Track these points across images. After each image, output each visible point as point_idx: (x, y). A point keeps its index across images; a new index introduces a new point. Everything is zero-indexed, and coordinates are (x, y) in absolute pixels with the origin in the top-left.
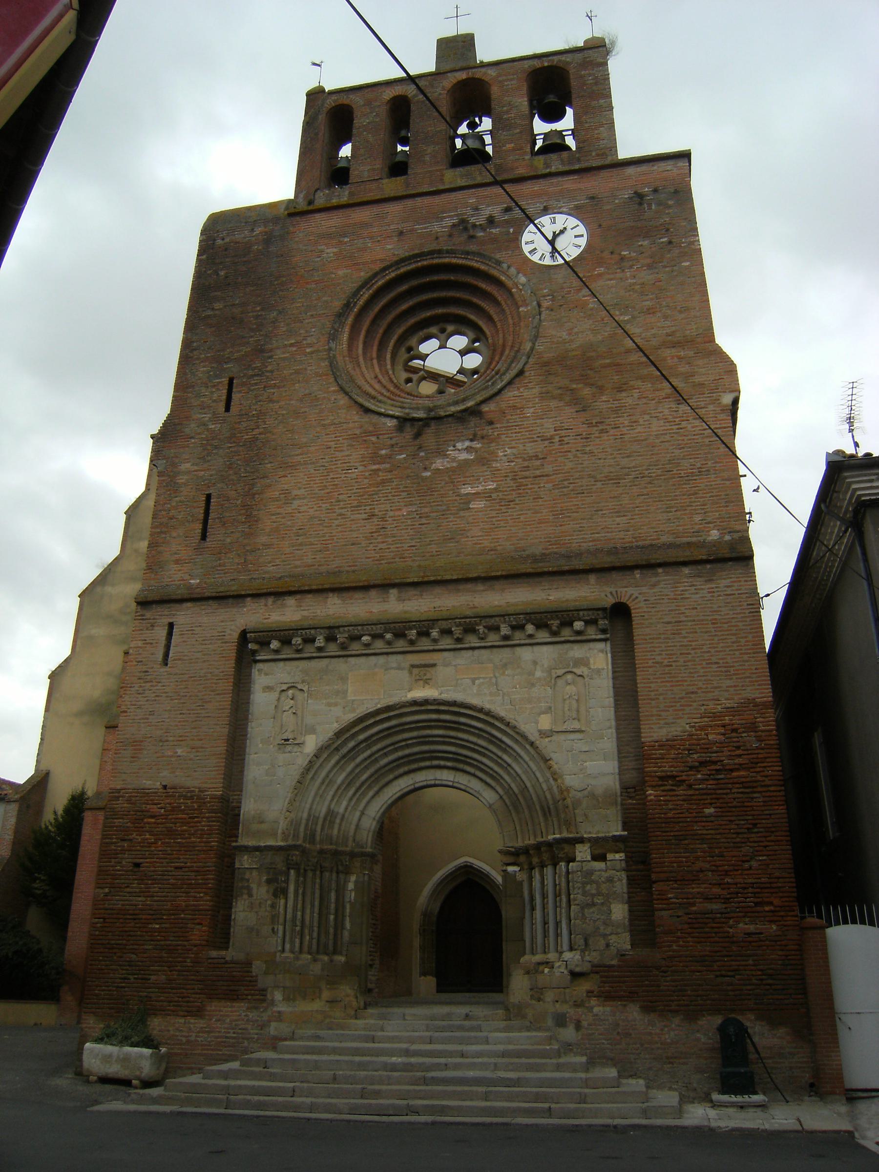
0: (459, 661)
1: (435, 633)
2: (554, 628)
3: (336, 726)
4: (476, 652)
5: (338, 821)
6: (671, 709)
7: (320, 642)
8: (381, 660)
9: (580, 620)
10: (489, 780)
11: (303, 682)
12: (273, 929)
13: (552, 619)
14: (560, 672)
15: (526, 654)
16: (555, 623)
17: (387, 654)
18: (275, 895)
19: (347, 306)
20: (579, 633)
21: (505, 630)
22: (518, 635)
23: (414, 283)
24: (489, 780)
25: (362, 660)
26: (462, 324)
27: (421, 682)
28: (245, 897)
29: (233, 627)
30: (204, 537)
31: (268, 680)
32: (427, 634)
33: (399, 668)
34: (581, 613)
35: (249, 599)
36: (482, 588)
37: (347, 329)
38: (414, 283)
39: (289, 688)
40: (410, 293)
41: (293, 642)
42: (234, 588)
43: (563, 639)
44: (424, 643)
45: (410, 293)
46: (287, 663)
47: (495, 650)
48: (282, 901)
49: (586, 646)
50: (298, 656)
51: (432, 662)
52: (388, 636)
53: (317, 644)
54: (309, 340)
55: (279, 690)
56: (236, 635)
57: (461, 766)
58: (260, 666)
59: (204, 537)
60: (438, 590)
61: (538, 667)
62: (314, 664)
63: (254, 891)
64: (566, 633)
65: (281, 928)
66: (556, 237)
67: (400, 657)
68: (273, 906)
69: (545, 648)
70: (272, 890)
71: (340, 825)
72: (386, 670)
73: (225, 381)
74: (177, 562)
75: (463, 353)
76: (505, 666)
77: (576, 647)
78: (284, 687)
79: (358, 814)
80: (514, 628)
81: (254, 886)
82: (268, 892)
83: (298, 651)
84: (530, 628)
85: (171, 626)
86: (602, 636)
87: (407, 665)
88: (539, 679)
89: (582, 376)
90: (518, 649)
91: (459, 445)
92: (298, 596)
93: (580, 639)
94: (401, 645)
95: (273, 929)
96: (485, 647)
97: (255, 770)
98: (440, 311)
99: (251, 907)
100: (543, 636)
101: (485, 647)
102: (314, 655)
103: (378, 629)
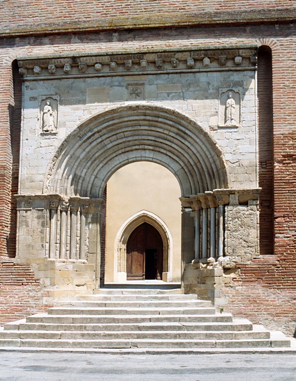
0: (159, 82)
1: (144, 63)
2: (223, 61)
3: (79, 123)
4: (170, 75)
5: (81, 181)
6: (292, 115)
7: (67, 68)
8: (108, 79)
9: (239, 56)
10: (175, 157)
11: (56, 94)
12: (42, 245)
13: (221, 54)
14: (224, 90)
15: (203, 78)
16: (223, 57)
17: (112, 76)
18: (43, 225)
20: (238, 65)
21: (191, 62)
22: (198, 64)
24: (175, 157)
25: (95, 80)
27: (134, 95)
28: (24, 227)
29: (8, 58)
32: (139, 64)
33: (120, 85)
34: (241, 51)
35: (18, 39)
36: (175, 34)
39: (47, 99)
41: (49, 68)
42: (7, 31)
43: (227, 69)
44: (136, 70)
46: (45, 82)
47: (182, 75)
48: (48, 229)
49: (241, 74)
50: (52, 77)
51: (141, 82)
52: (113, 64)
53: (65, 69)
55: (40, 100)
56: (10, 64)
57: (158, 149)
58: (27, 84)
61: (210, 86)
62: (64, 82)
63: (30, 224)
64: (230, 64)
65: (47, 245)
67: (120, 78)
68: (42, 232)
69: (215, 74)
70: (40, 223)
71: (82, 183)
72: (111, 87)
76: (189, 85)
77: (235, 74)
78: (44, 98)
79: (93, 177)
80: (195, 60)
81: (29, 221)
82: (38, 223)
83: (52, 74)
84: (207, 61)
86: (253, 68)
87: (125, 84)
88: (211, 94)
90: (198, 74)
92: (51, 37)
93: (237, 69)
95: (42, 245)
96: (177, 73)
99: (28, 233)
100: (215, 66)
101: (177, 73)
102: (63, 76)
103: (106, 59)
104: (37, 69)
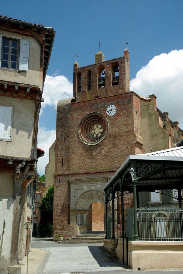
19: (81, 124)
23: (91, 118)
26: (100, 124)
30: (63, 165)
31: (73, 187)
37: (81, 128)
38: (91, 118)
40: (91, 119)
45: (91, 119)
54: (75, 130)
59: (63, 165)
60: (94, 174)
66: (112, 110)
73: (63, 137)
74: (59, 169)
75: (100, 129)
84: (105, 180)
85: (59, 179)
89: (115, 137)
91: (97, 150)
94: (89, 183)
97: (72, 201)
98: (95, 122)
104: (73, 183)
